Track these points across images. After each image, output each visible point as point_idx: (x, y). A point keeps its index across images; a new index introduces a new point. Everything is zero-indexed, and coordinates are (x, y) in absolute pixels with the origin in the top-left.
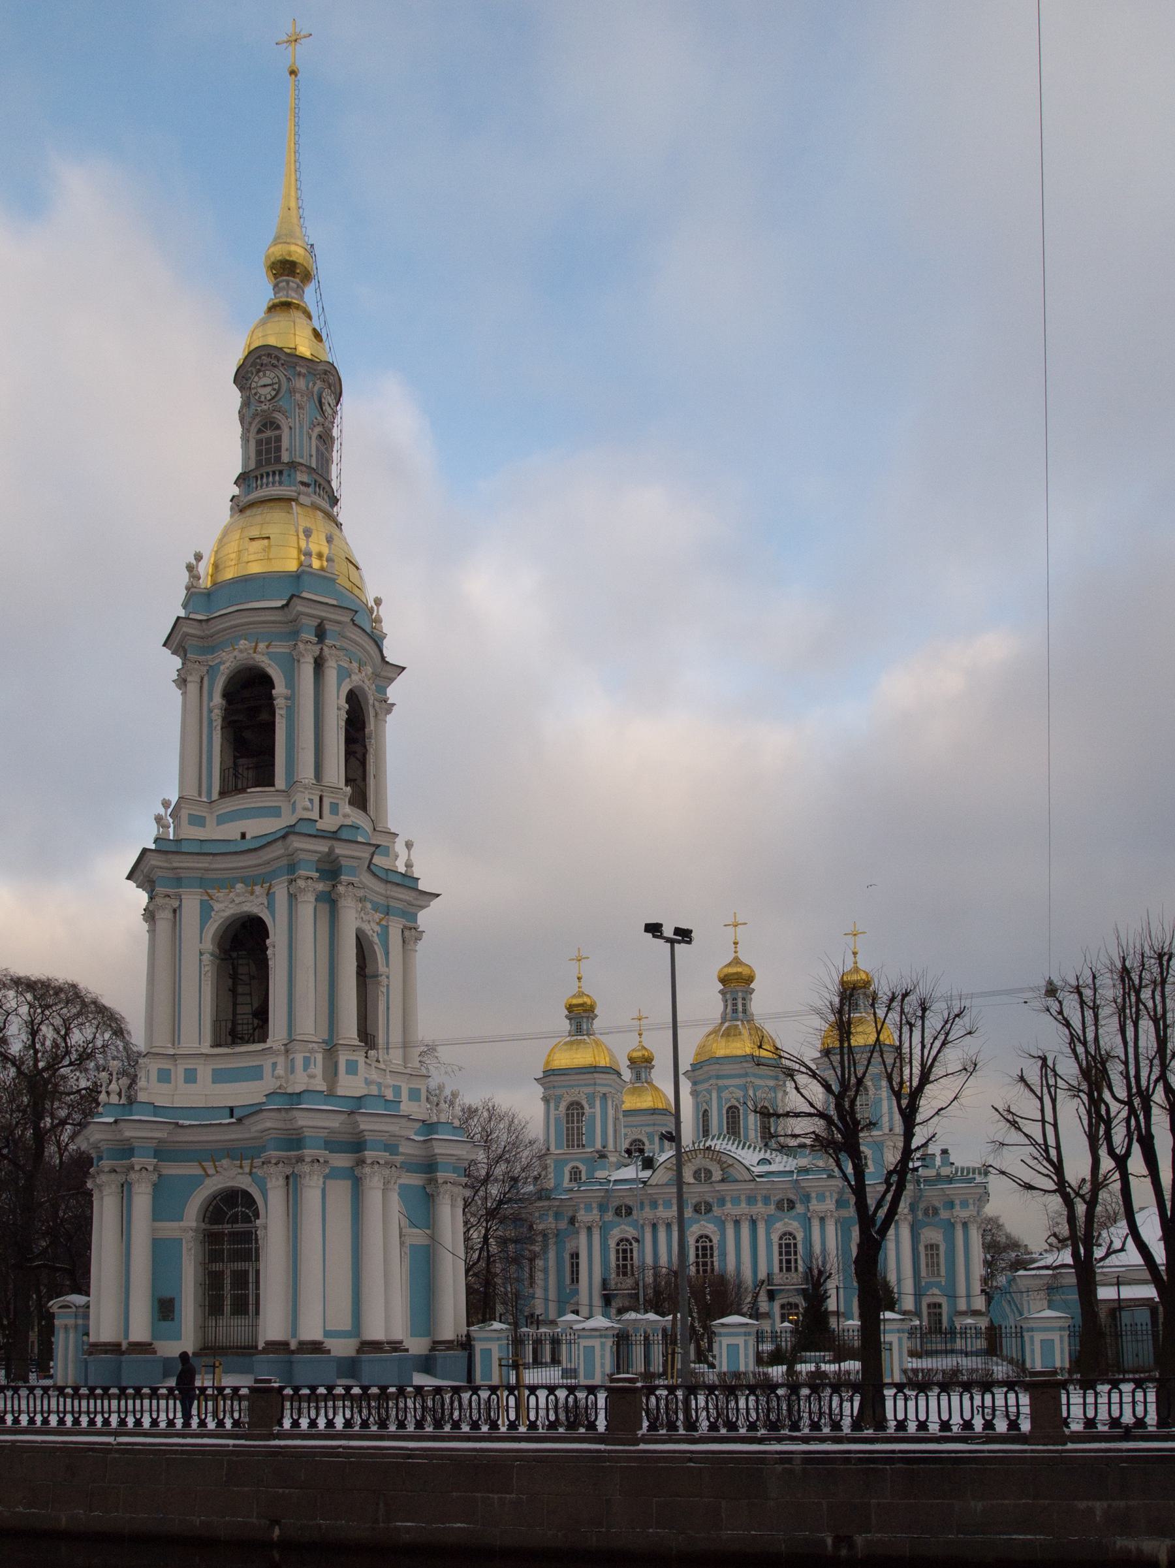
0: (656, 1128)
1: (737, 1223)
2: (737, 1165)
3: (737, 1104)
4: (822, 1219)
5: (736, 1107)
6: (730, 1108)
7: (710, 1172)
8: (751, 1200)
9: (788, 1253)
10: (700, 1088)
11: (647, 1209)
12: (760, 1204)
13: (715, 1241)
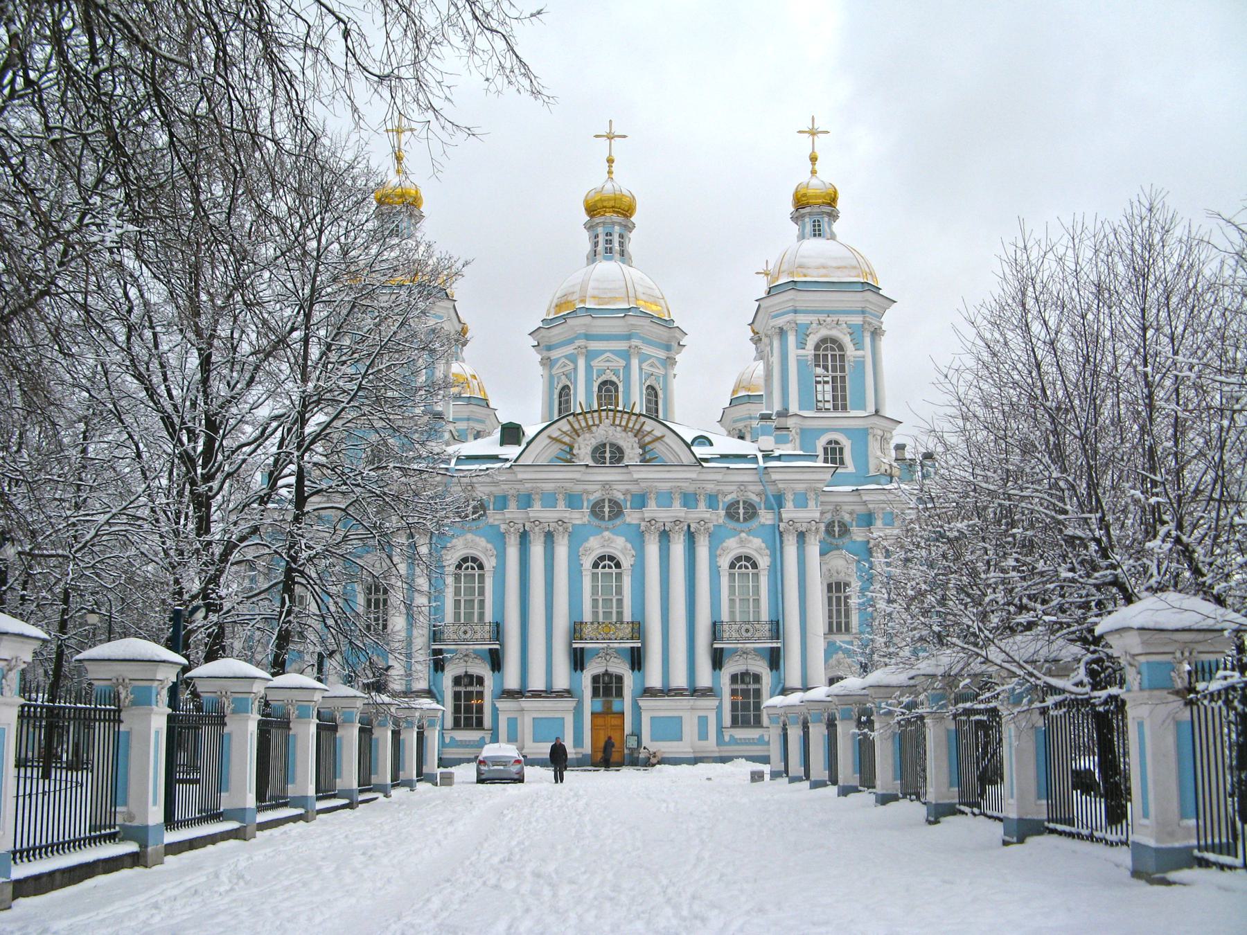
0: (472, 424)
1: (665, 536)
2: (670, 439)
3: (614, 379)
4: (801, 536)
6: (605, 383)
8: (689, 500)
10: (555, 354)
12: (702, 505)
13: (626, 563)
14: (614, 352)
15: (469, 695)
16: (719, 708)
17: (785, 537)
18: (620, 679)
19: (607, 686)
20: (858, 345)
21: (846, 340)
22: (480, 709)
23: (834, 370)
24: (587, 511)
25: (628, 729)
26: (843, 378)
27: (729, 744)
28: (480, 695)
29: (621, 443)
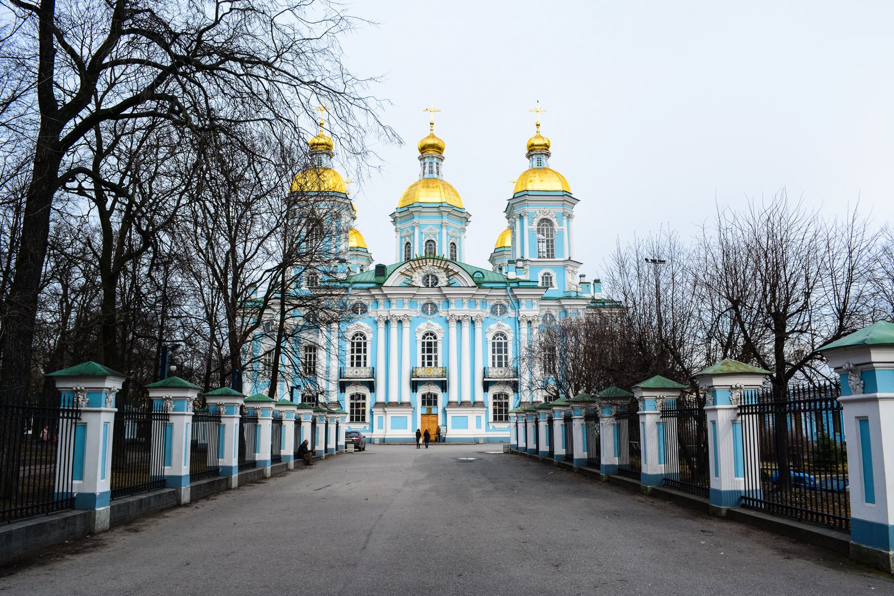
5: (433, 241)
6: (428, 241)
7: (437, 279)
9: (500, 351)
11: (381, 308)
12: (479, 308)
15: (358, 405)
18: (436, 396)
19: (429, 401)
20: (560, 224)
21: (554, 220)
22: (364, 411)
23: (547, 236)
24: (419, 309)
25: (440, 424)
26: (552, 241)
28: (364, 405)
29: (437, 275)
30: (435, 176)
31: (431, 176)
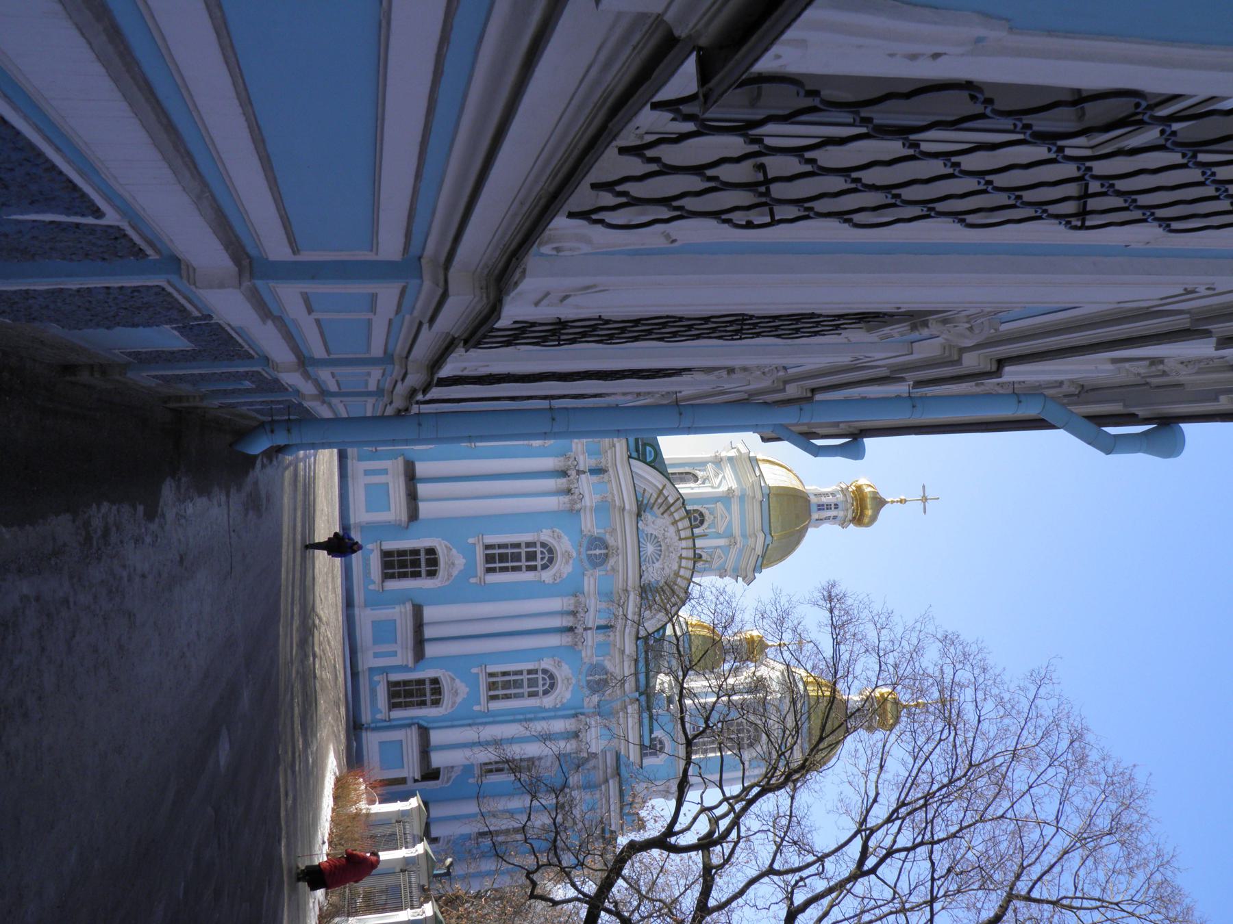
4: (576, 735)
14: (730, 522)
16: (404, 668)
17: (573, 720)
27: (370, 680)
30: (815, 516)
31: (814, 508)
